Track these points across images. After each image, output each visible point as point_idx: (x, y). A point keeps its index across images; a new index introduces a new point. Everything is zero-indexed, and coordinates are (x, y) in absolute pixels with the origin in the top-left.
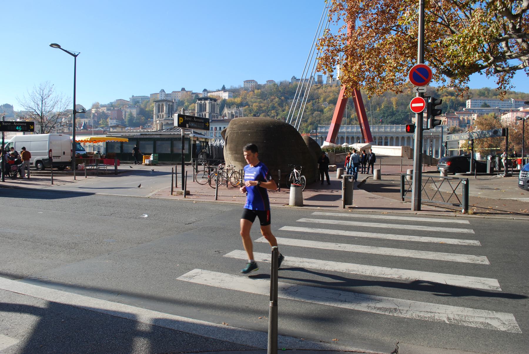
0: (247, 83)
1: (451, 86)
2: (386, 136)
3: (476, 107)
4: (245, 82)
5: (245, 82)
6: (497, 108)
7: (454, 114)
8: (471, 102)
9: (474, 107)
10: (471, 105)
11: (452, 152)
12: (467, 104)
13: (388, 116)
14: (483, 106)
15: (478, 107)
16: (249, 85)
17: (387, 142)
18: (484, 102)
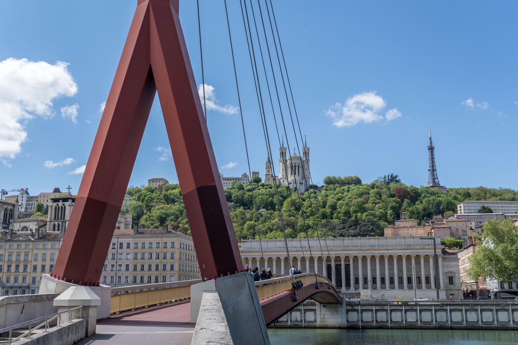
0: (153, 182)
1: (433, 187)
2: (347, 255)
3: (471, 213)
4: (150, 181)
5: (150, 181)
6: (501, 213)
7: (443, 223)
8: (464, 206)
9: (469, 213)
10: (464, 210)
11: (452, 279)
12: (459, 209)
13: (350, 226)
14: (480, 211)
15: (475, 213)
16: (155, 185)
17: (349, 265)
18: (482, 205)
